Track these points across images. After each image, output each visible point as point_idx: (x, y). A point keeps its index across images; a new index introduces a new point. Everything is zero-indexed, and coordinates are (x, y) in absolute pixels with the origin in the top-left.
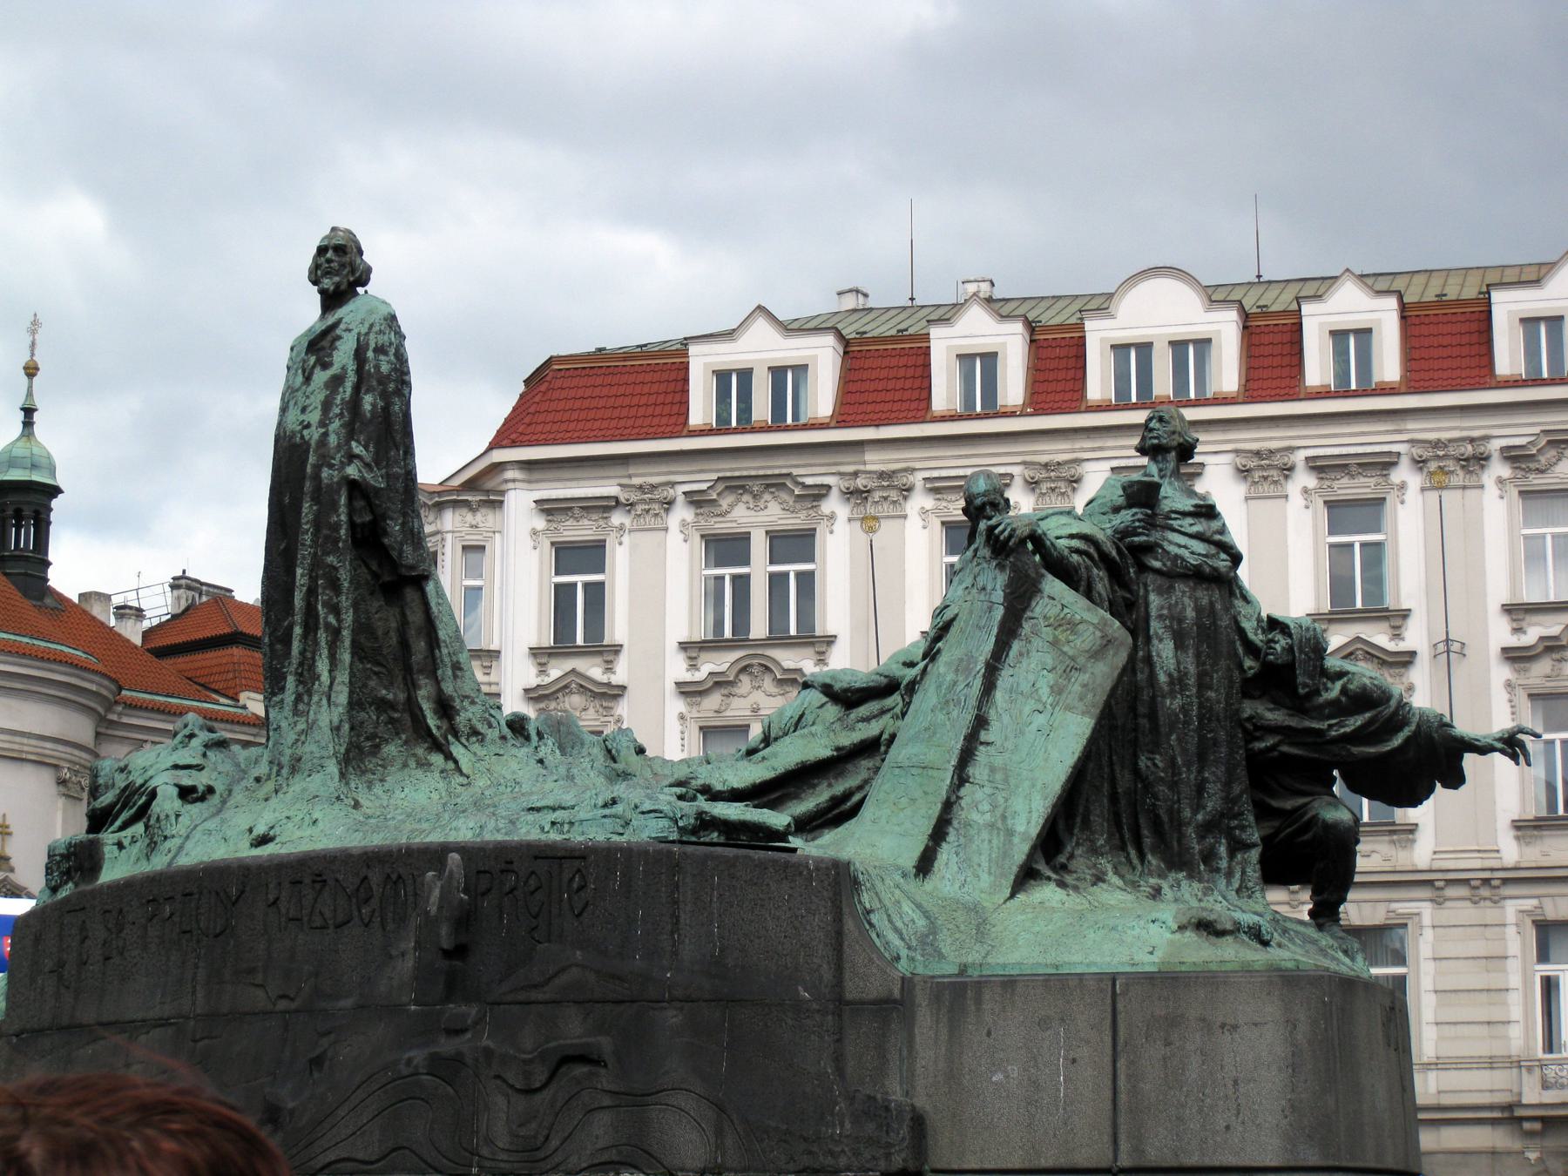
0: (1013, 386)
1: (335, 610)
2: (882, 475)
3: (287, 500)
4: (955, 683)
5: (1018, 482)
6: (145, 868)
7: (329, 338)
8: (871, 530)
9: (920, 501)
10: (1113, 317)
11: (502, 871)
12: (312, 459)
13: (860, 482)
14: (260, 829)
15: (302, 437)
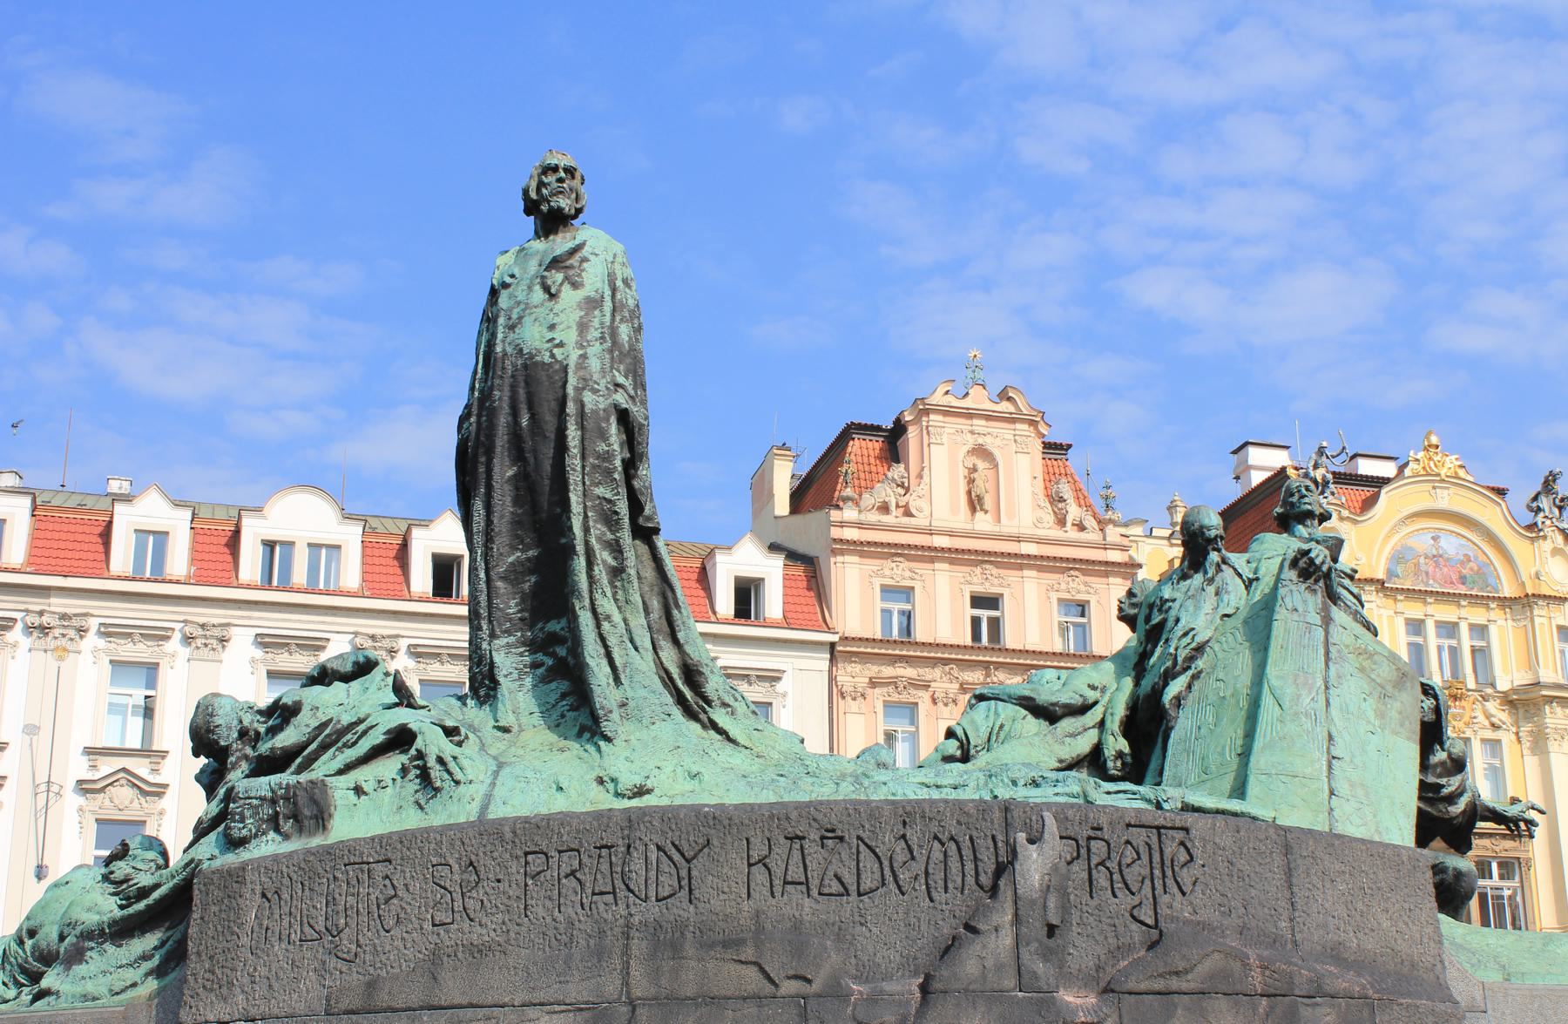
0: (179, 560)
1: (616, 548)
2: (64, 617)
3: (524, 422)
4: (1299, 696)
5: (177, 636)
6: (412, 820)
7: (577, 257)
8: (61, 659)
9: (92, 640)
10: (265, 518)
11: (1090, 838)
12: (572, 381)
13: (45, 620)
14: (628, 780)
15: (553, 356)
